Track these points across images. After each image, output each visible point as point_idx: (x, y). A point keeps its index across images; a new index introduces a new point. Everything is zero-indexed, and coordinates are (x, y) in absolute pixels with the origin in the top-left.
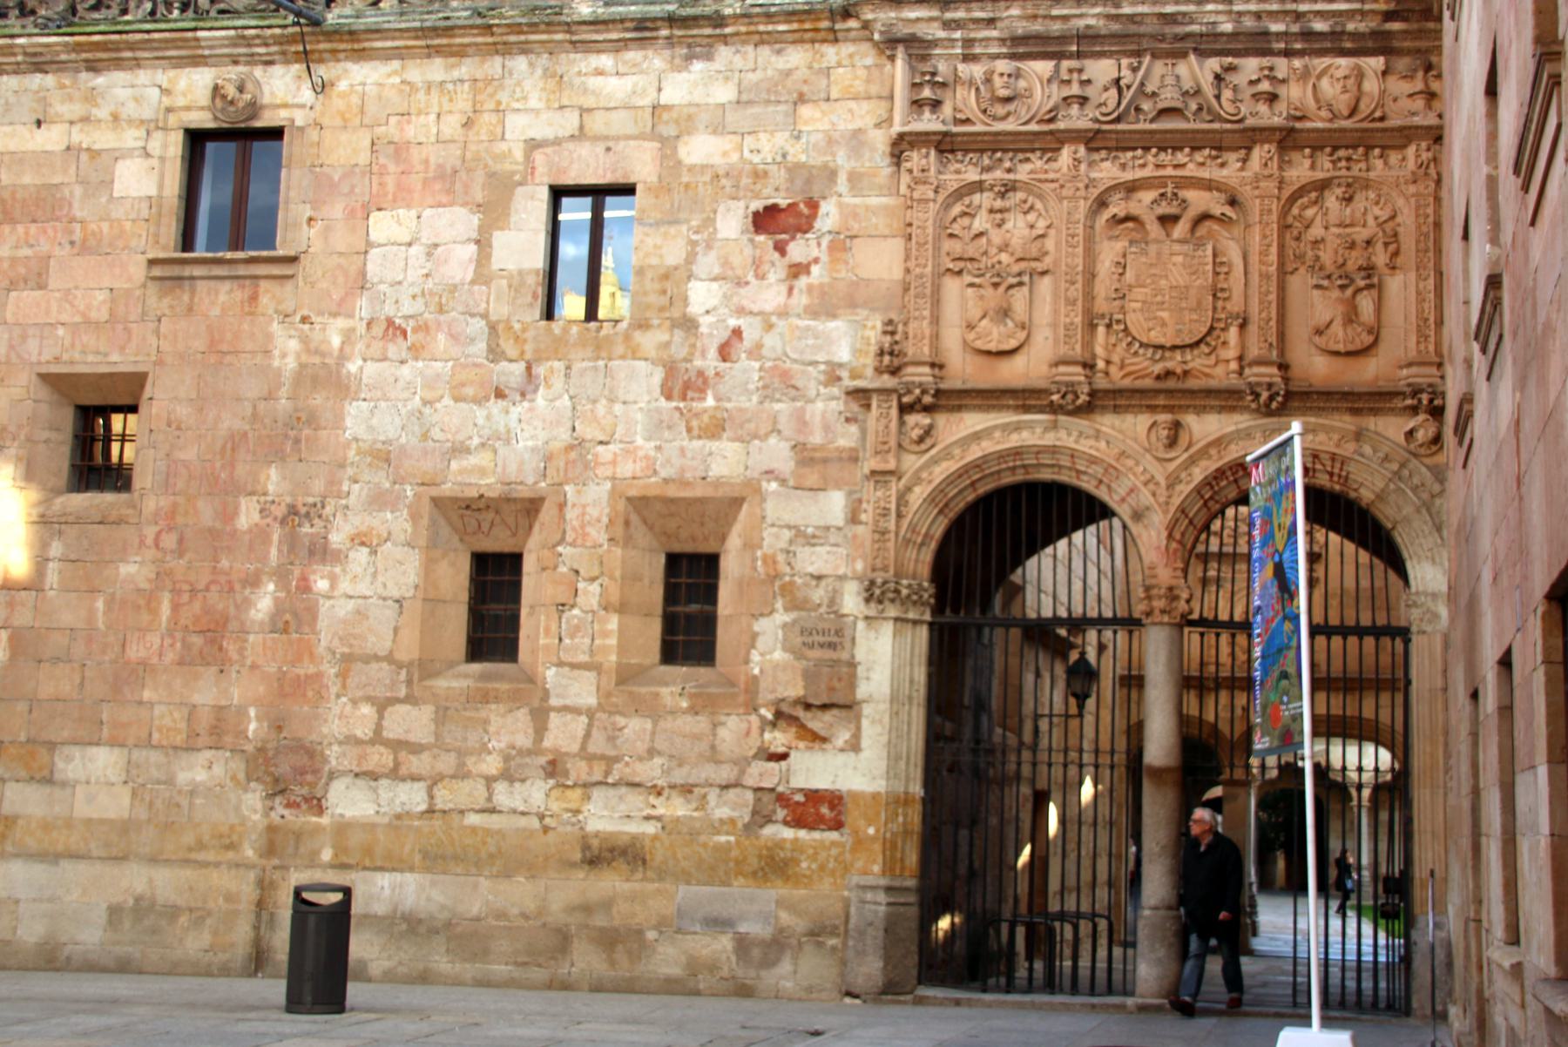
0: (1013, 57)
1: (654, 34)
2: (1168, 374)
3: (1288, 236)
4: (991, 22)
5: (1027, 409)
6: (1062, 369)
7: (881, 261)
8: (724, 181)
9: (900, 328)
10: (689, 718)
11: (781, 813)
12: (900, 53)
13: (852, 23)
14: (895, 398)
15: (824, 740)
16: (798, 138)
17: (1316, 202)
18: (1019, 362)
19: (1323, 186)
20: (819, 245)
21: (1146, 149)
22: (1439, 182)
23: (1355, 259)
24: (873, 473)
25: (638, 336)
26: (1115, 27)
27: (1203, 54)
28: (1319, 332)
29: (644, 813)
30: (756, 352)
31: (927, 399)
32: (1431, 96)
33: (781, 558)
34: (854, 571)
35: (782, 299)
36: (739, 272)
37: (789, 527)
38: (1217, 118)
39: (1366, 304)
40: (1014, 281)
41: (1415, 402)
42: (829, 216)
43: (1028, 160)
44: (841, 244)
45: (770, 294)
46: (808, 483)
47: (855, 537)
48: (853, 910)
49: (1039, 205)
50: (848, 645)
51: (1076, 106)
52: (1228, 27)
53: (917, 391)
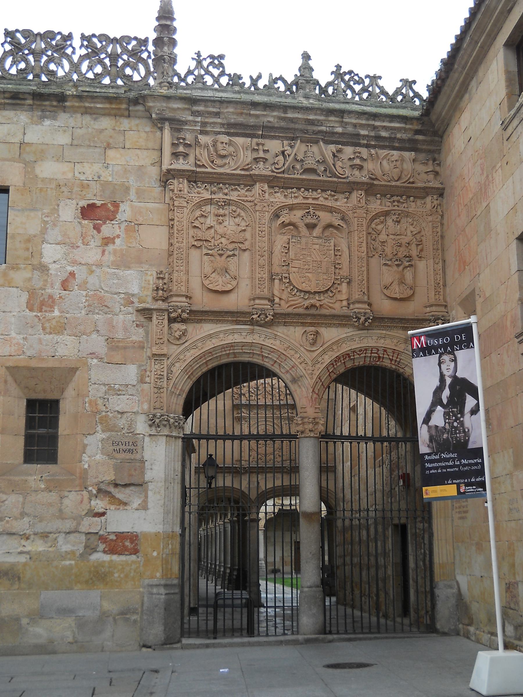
0: (228, 134)
1: (23, 102)
2: (313, 306)
3: (369, 238)
5: (237, 323)
6: (257, 301)
7: (155, 239)
8: (63, 189)
9: (167, 276)
10: (45, 494)
11: (102, 547)
12: (167, 126)
13: (140, 108)
14: (166, 313)
15: (125, 504)
16: (107, 167)
17: (382, 222)
18: (232, 297)
19: (386, 214)
20: (120, 228)
21: (299, 189)
22: (442, 216)
23: (402, 252)
24: (154, 355)
25: (12, 274)
26: (283, 124)
27: (327, 142)
28: (386, 288)
29: (19, 550)
30: (84, 286)
31: (185, 315)
32: (437, 174)
33: (100, 402)
34: (143, 409)
35: (98, 257)
36: (74, 241)
37: (104, 385)
38: (335, 176)
39: (408, 275)
40: (231, 253)
42: (125, 212)
43: (236, 189)
44: (133, 227)
45: (91, 254)
46: (115, 360)
47: (143, 390)
48: (146, 599)
49: (243, 214)
50: (139, 451)
51: (262, 163)
52: (340, 130)
53: (180, 311)
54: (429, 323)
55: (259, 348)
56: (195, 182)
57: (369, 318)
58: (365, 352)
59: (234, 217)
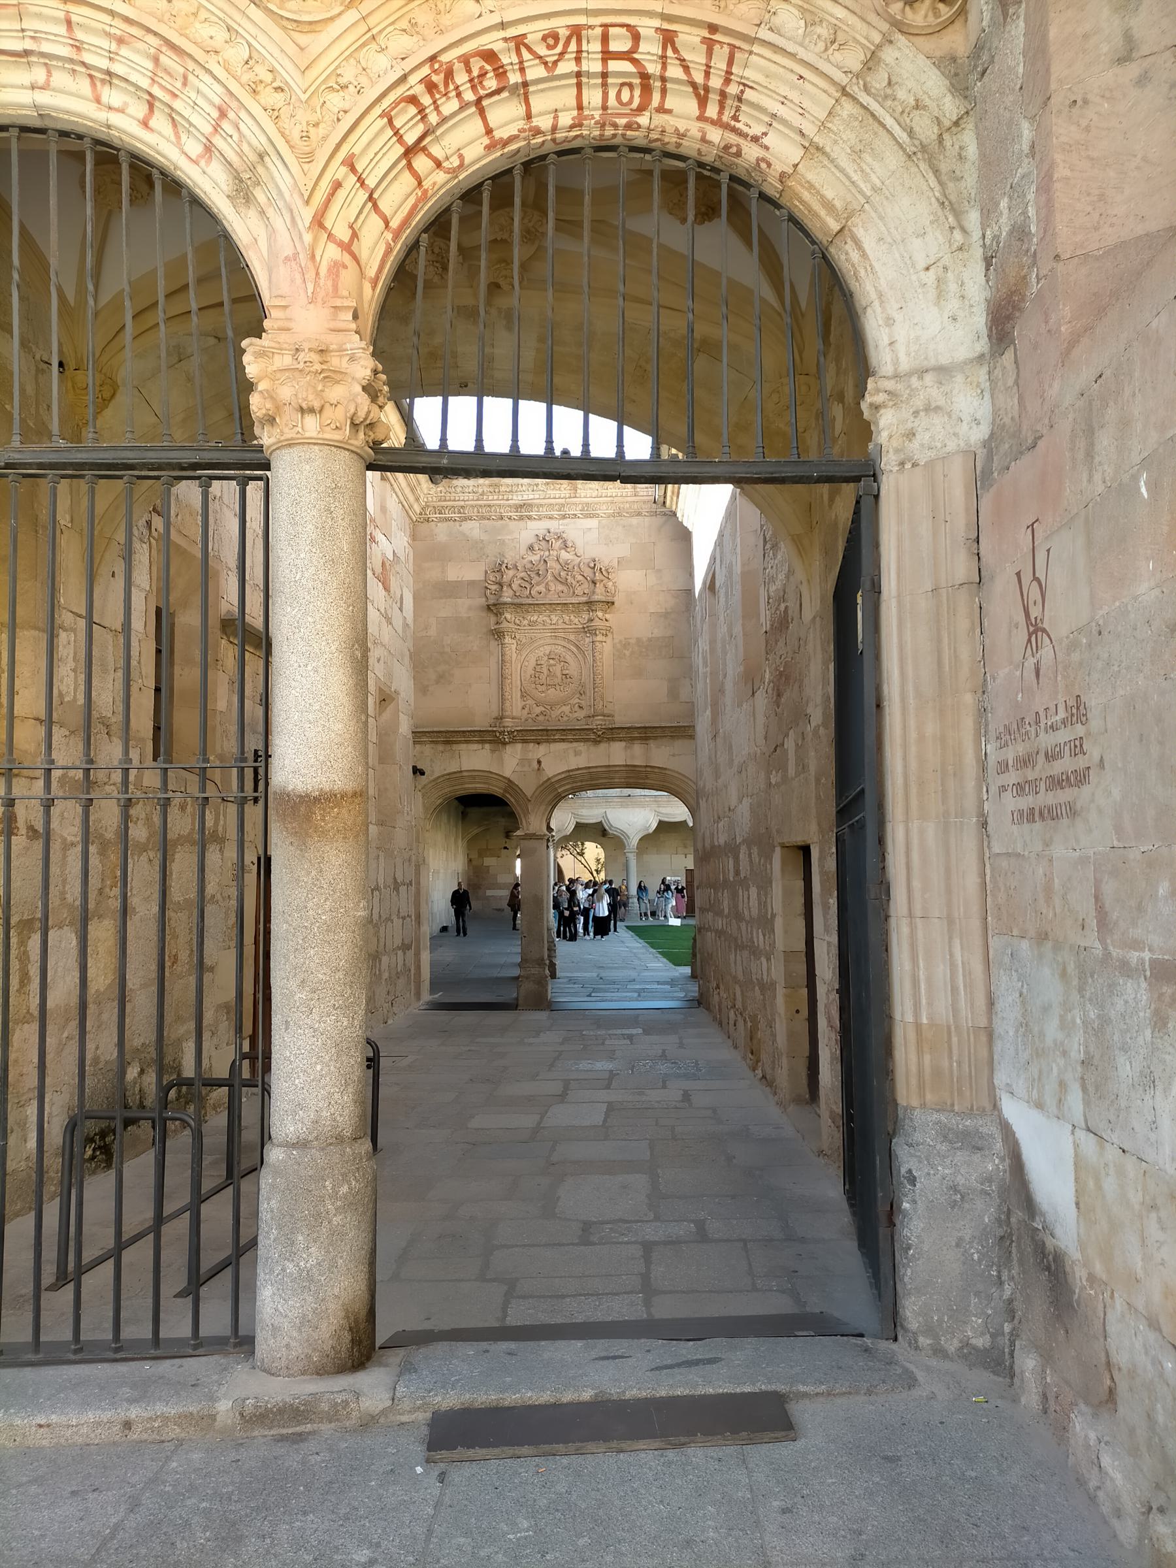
55: (55, 20)
58: (573, 47)
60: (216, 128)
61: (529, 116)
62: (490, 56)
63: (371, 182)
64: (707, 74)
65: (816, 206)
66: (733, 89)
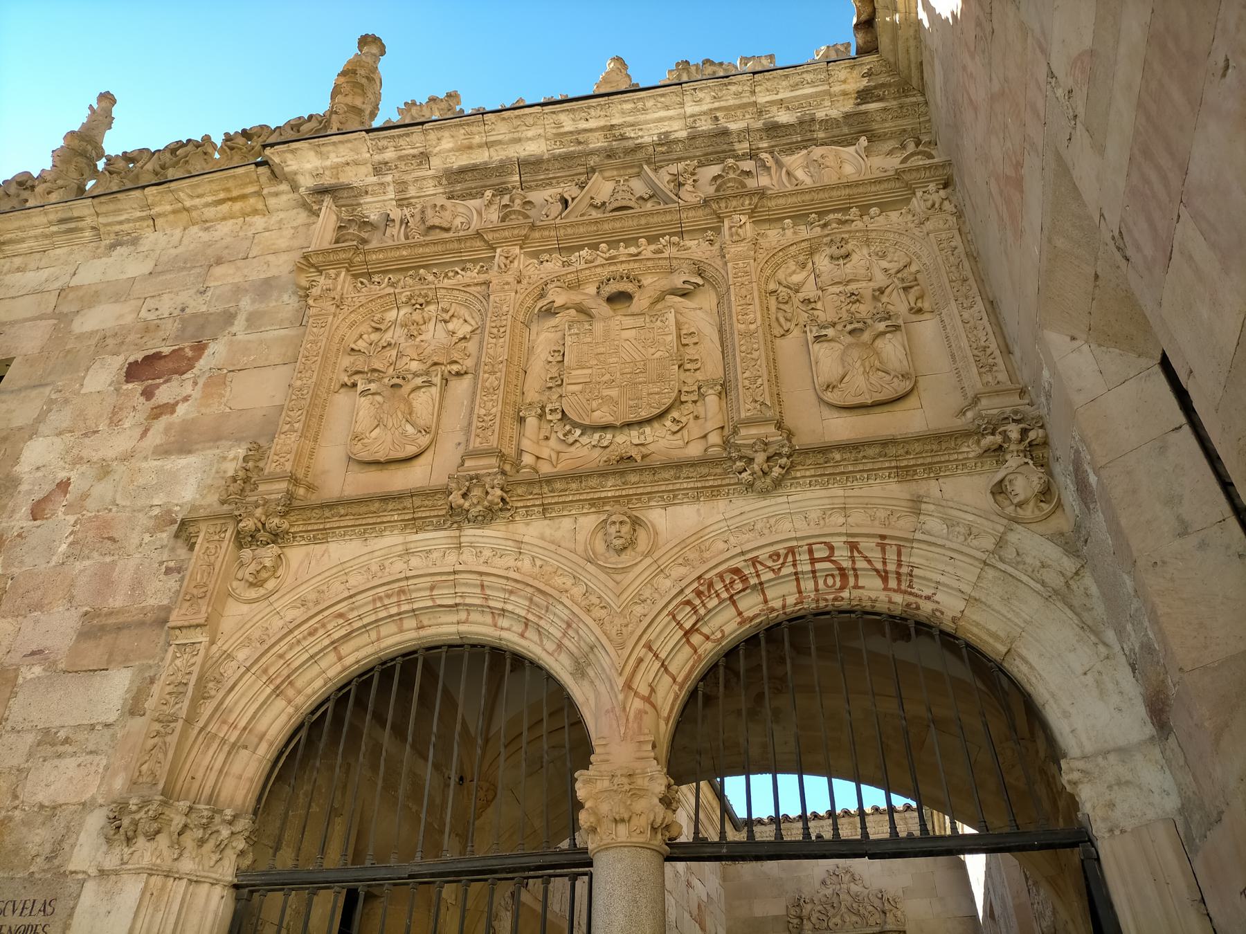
4: (424, 157)
5: (415, 524)
20: (195, 383)
28: (829, 387)
41: (998, 439)
54: (978, 442)
55: (475, 586)
56: (369, 275)
57: (780, 455)
58: (790, 558)
59: (446, 322)
60: (564, 634)
61: (766, 601)
62: (736, 571)
63: (663, 655)
64: (884, 563)
65: (985, 637)
66: (904, 570)
